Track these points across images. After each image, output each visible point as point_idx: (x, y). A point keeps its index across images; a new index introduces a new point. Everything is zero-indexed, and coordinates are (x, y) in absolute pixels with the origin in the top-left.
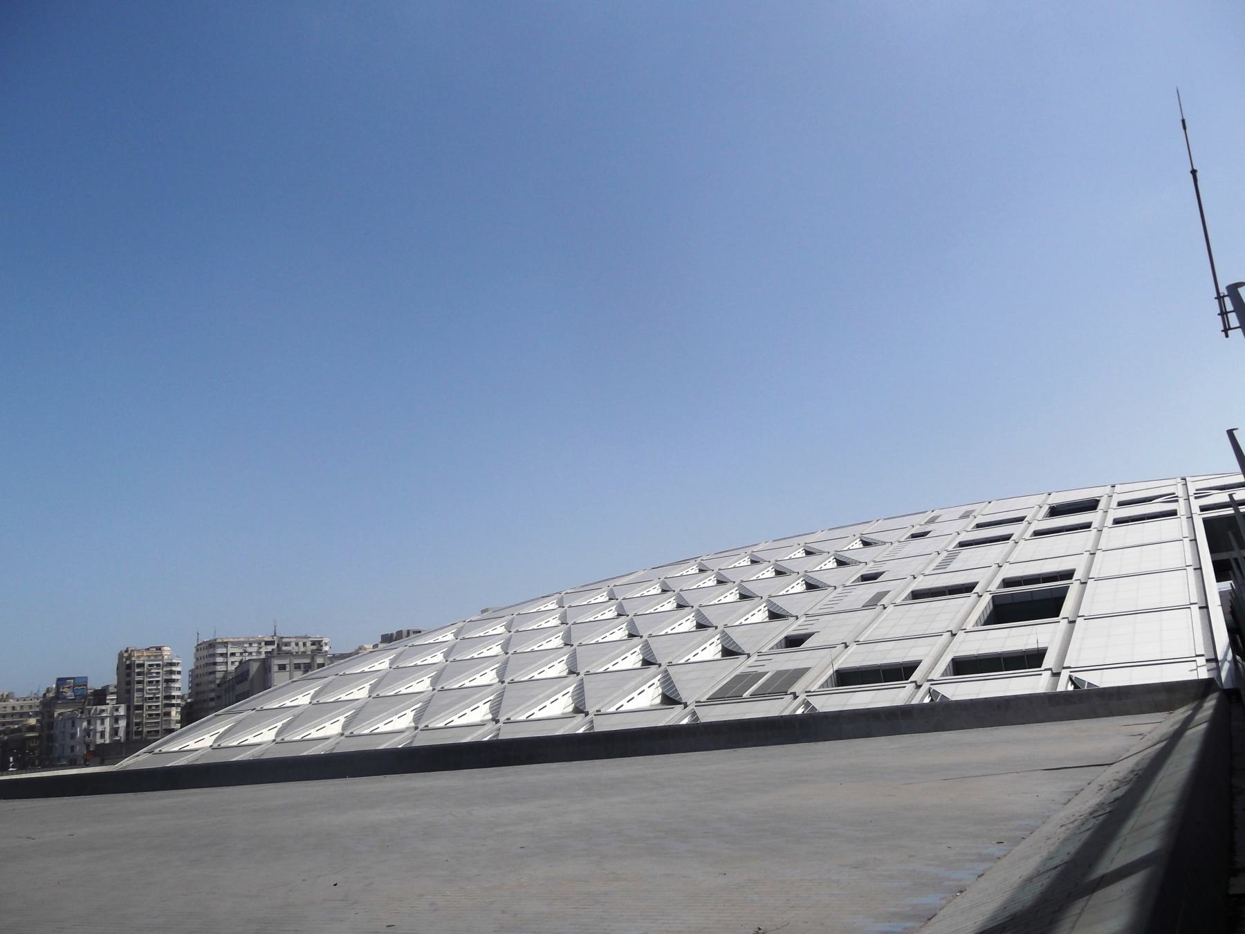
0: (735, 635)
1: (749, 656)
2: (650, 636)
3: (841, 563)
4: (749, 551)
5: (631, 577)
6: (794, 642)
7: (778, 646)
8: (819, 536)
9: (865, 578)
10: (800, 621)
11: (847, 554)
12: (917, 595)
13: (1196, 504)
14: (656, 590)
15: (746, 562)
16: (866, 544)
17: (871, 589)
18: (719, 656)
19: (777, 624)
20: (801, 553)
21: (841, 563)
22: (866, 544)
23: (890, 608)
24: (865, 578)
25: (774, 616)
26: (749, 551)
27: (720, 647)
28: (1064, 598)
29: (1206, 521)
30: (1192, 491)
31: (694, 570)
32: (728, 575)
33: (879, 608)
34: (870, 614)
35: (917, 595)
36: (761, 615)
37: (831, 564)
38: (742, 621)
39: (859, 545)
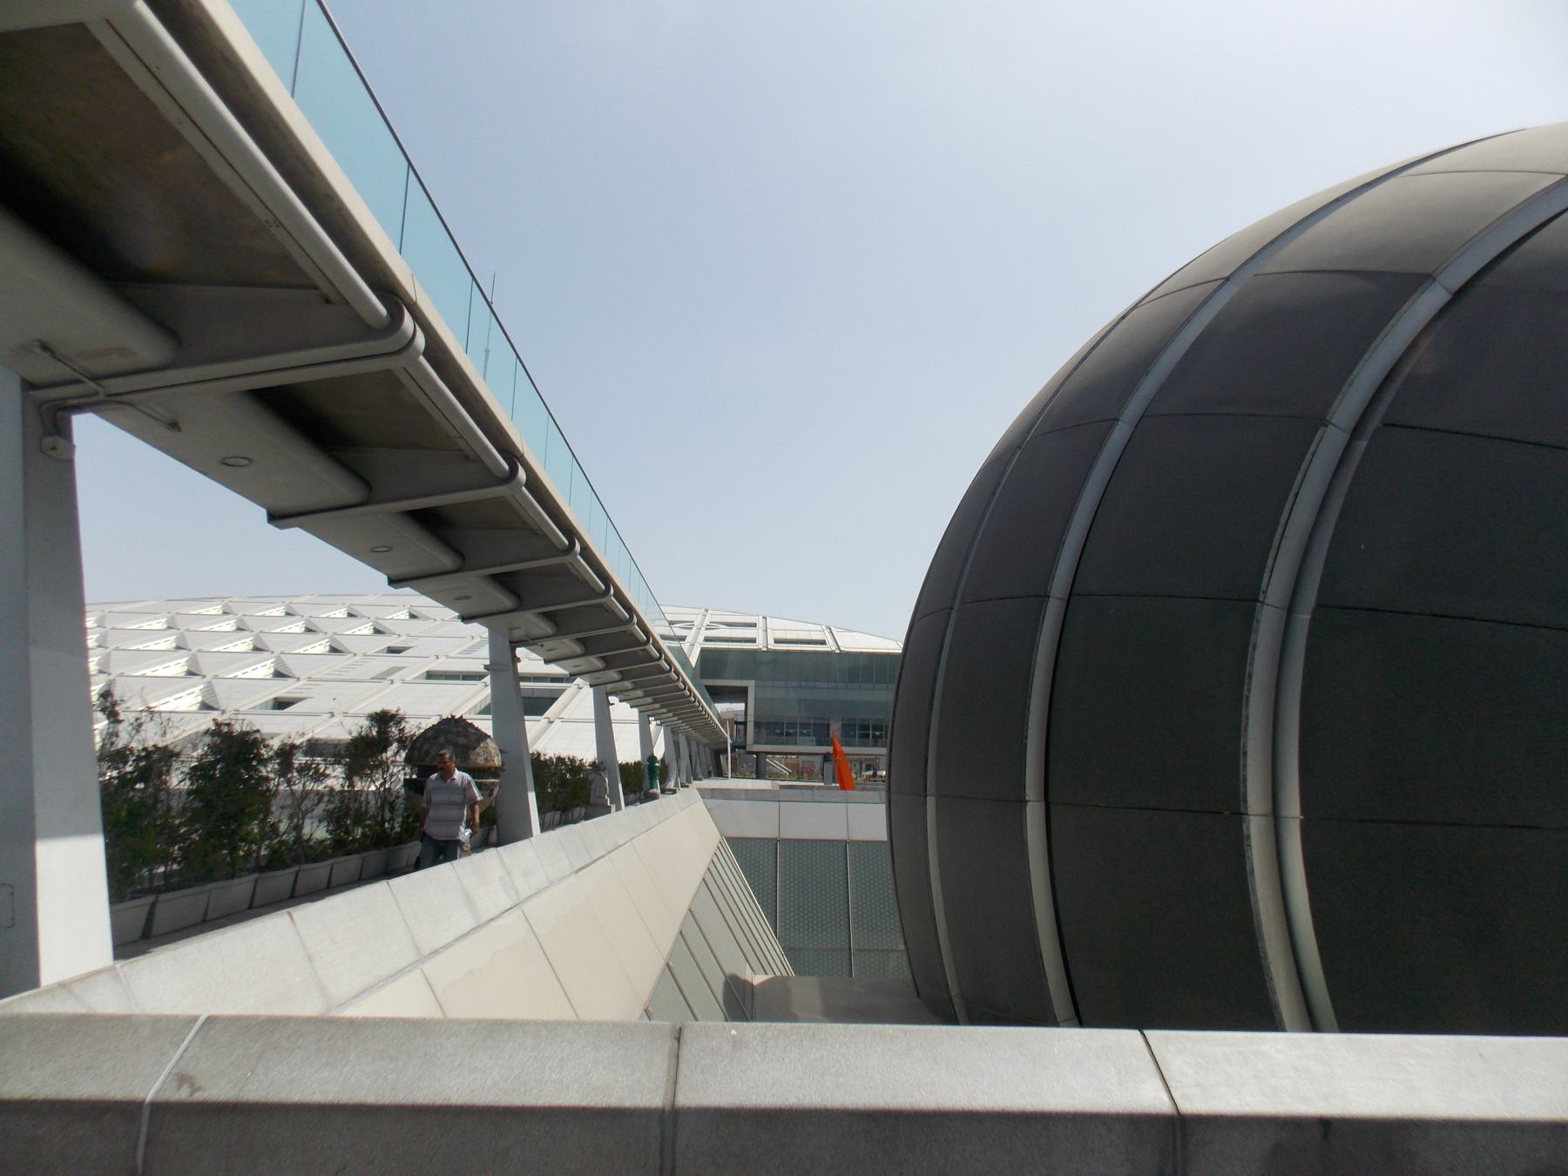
0: (221, 689)
1: (223, 712)
2: (121, 675)
3: (377, 631)
4: (287, 601)
5: (135, 606)
6: (281, 704)
7: (262, 706)
8: (369, 599)
9: (392, 651)
10: (300, 683)
11: (385, 623)
12: (431, 675)
13: (704, 633)
14: (159, 624)
15: (279, 611)
16: (413, 616)
17: (395, 660)
18: (195, 708)
19: (280, 682)
20: (341, 613)
21: (377, 631)
22: (413, 616)
23: (398, 684)
24: (392, 651)
25: (278, 674)
26: (287, 601)
27: (200, 699)
28: (554, 700)
29: (703, 650)
30: (707, 622)
31: (216, 610)
32: (250, 623)
33: (386, 682)
34: (375, 686)
35: (431, 675)
36: (264, 669)
37: (367, 629)
38: (239, 674)
39: (404, 615)
